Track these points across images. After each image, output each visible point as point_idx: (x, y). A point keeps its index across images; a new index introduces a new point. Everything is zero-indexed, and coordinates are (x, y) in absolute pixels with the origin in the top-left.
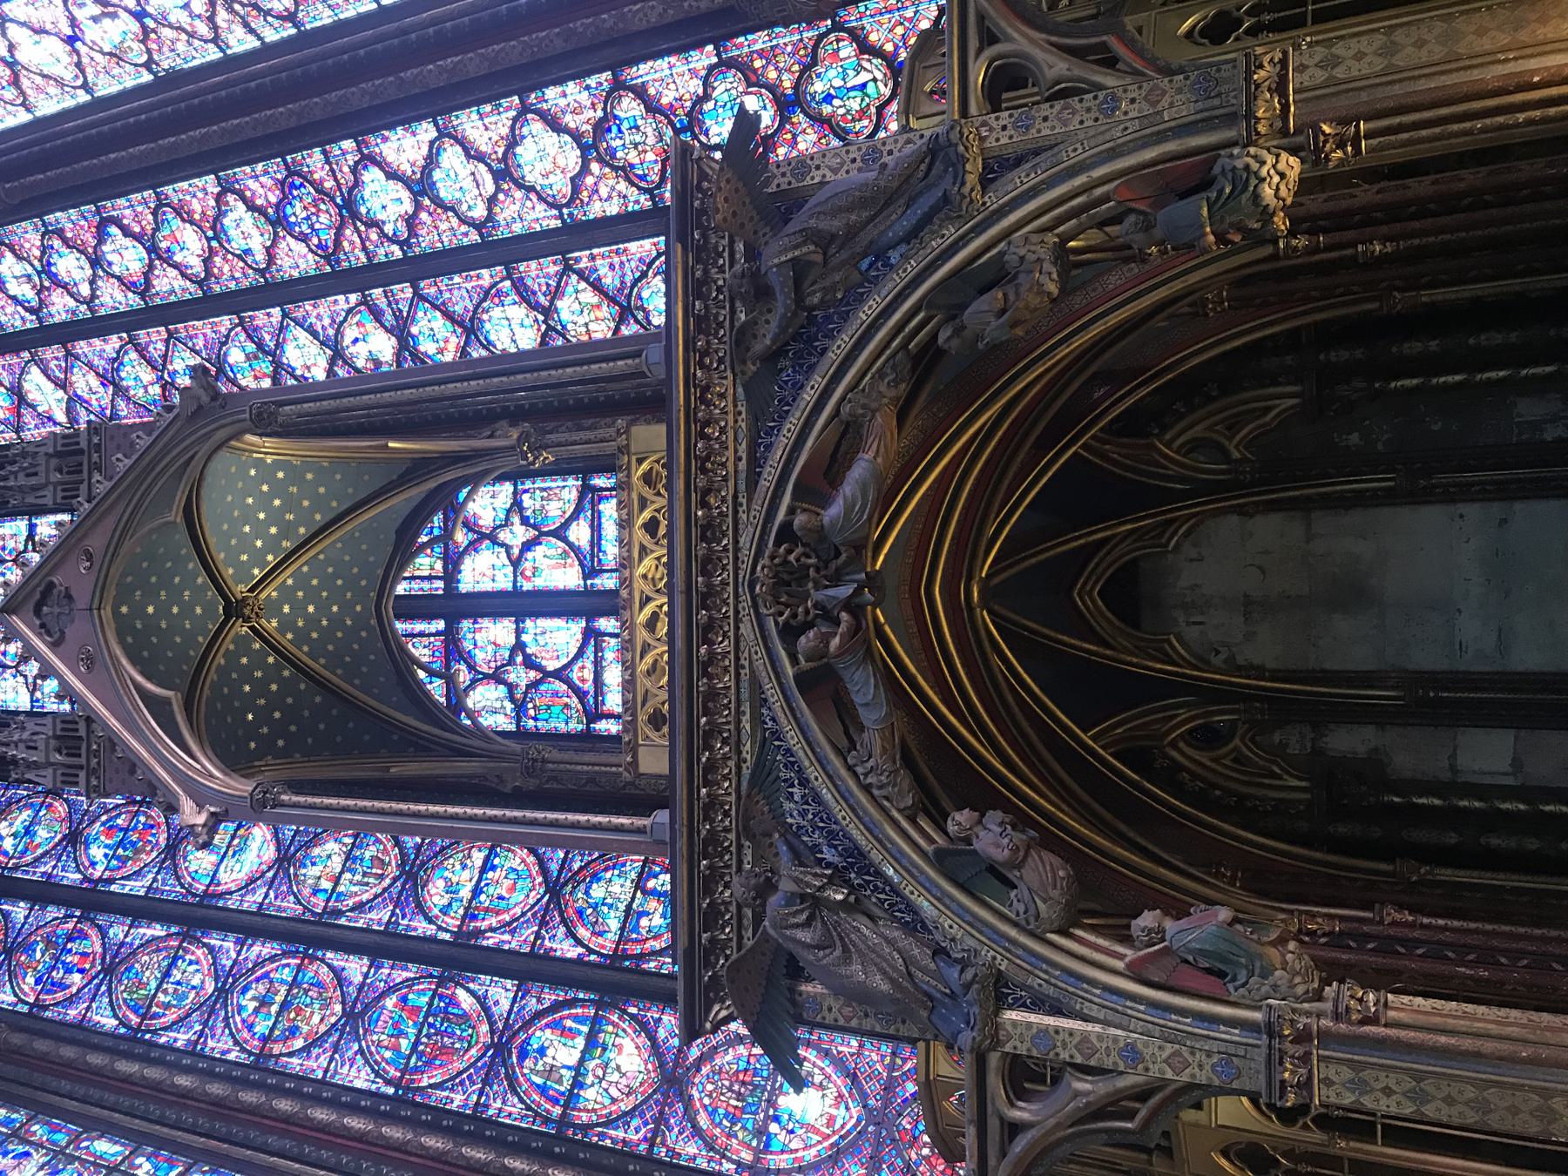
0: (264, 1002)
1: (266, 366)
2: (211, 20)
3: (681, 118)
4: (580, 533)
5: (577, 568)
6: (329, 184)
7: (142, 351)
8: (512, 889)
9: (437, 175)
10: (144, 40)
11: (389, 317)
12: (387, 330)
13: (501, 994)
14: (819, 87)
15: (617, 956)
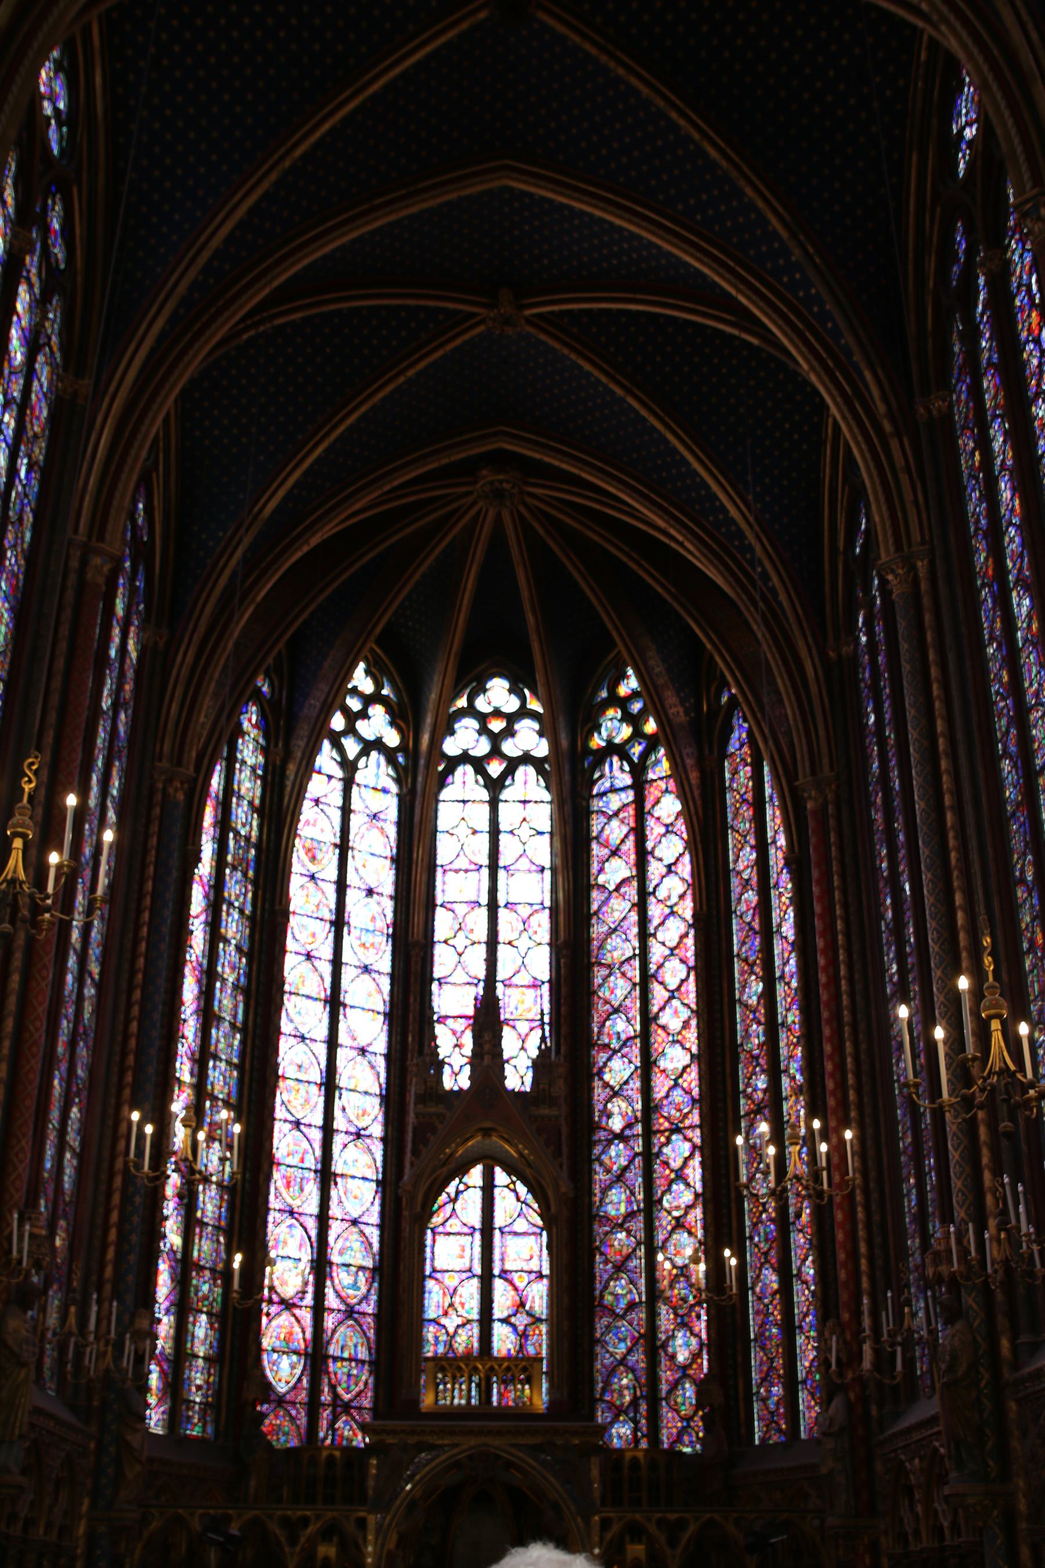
0: (300, 1067)
1: (615, 1044)
2: (749, 1097)
3: (686, 1319)
4: (521, 1225)
5: (503, 1224)
6: (687, 1122)
7: (629, 959)
8: (356, 1197)
9: (682, 1187)
10: (750, 1052)
11: (628, 1132)
12: (623, 1130)
13: (311, 1206)
14: (687, 1385)
15: (331, 1264)
